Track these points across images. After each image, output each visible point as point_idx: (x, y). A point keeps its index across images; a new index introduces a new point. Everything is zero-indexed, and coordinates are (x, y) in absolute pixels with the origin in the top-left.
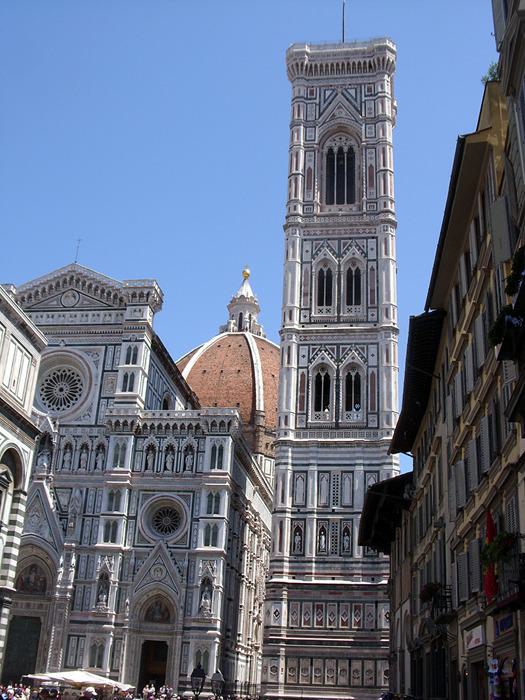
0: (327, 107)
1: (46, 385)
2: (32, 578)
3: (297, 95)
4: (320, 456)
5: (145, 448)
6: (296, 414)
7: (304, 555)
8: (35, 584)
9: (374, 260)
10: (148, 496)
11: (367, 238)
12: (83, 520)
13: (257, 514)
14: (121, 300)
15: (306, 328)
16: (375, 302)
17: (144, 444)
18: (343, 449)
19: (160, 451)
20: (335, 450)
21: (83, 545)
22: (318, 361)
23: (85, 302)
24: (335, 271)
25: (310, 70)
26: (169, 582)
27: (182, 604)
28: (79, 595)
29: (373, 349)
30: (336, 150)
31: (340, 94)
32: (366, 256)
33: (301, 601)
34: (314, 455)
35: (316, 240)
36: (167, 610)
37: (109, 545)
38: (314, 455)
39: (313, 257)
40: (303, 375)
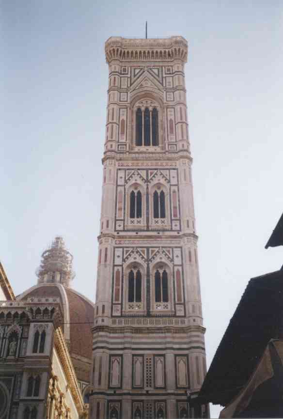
0: (137, 79)
3: (113, 70)
4: (133, 340)
6: (112, 304)
15: (121, 234)
16: (176, 216)
18: (154, 335)
20: (147, 335)
22: (131, 260)
24: (143, 191)
25: (123, 55)
29: (177, 252)
30: (143, 109)
31: (146, 71)
32: (169, 182)
35: (128, 169)
38: (129, 340)
39: (126, 182)
40: (118, 272)
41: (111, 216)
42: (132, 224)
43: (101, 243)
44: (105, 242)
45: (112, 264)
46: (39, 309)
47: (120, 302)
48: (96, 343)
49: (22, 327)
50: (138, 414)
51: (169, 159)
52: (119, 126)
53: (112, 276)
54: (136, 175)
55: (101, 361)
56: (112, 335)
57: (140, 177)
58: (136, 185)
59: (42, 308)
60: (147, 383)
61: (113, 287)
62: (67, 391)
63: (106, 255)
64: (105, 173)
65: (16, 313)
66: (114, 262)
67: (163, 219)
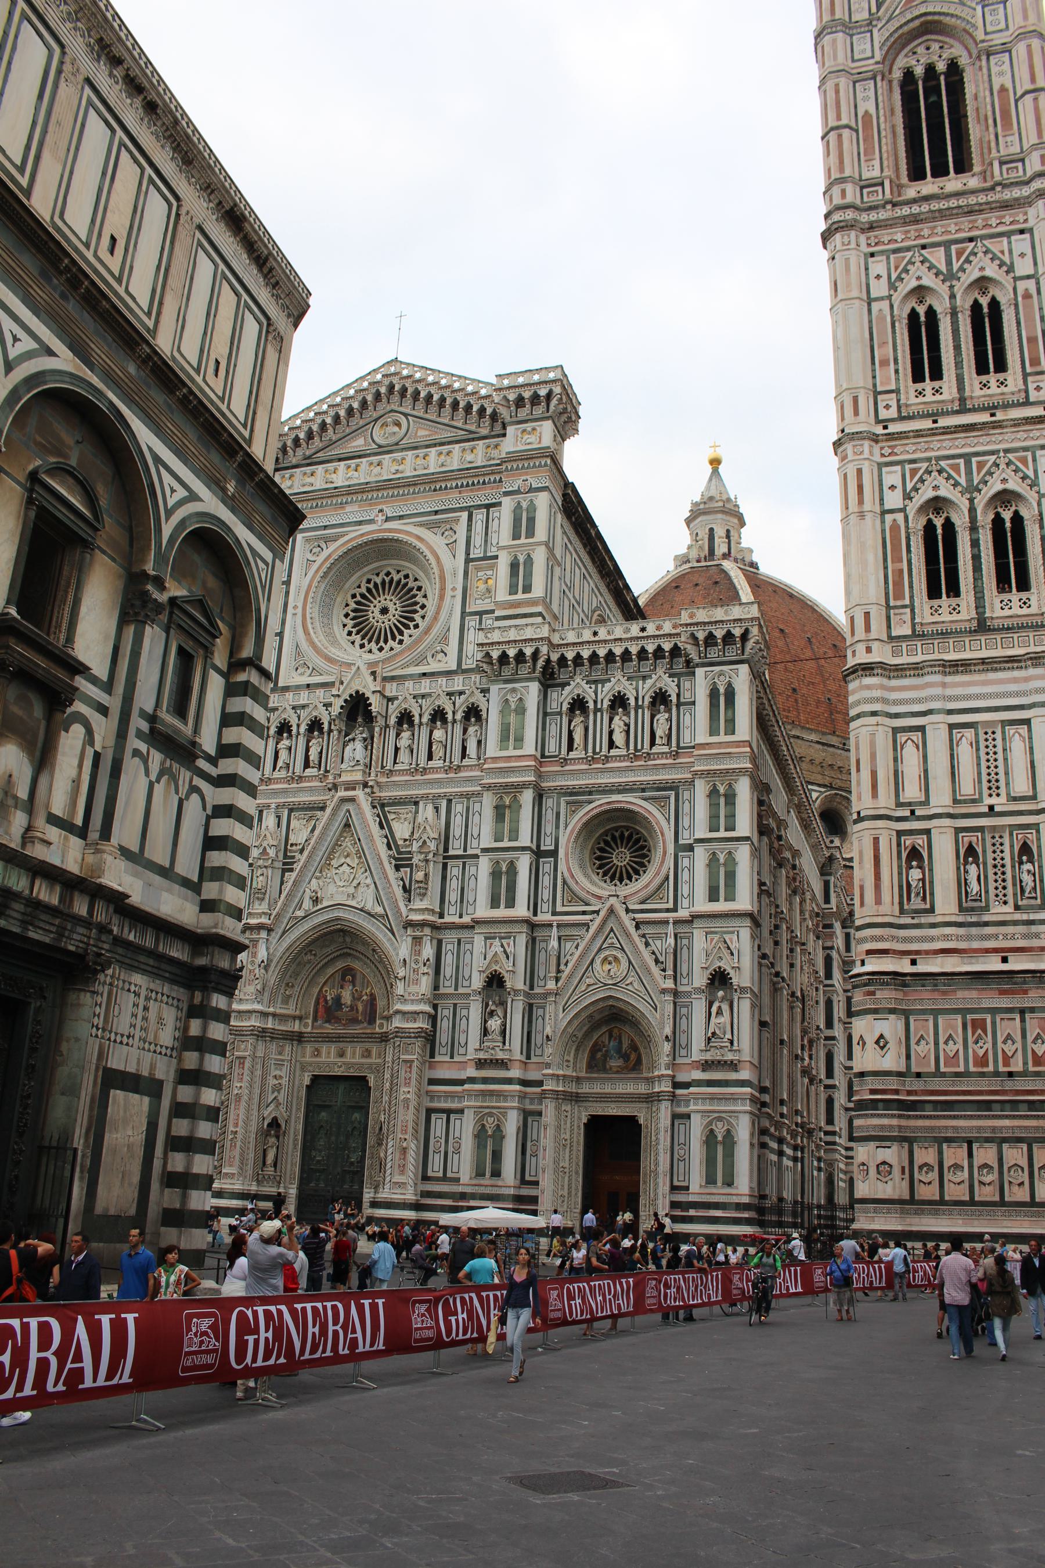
1: (353, 606)
2: (347, 997)
4: (949, 692)
5: (566, 706)
6: (888, 607)
7: (932, 910)
8: (352, 1008)
9: (1028, 277)
10: (580, 804)
11: (1008, 234)
12: (445, 866)
13: (796, 853)
14: (494, 417)
15: (893, 428)
17: (560, 699)
18: (1000, 675)
19: (596, 710)
20: (982, 677)
21: (447, 919)
22: (927, 493)
23: (421, 433)
24: (941, 307)
26: (635, 984)
27: (668, 1030)
28: (444, 1025)
32: (1010, 269)
33: (936, 1013)
34: (938, 691)
35: (895, 251)
36: (634, 1048)
37: (502, 912)
38: (938, 691)
39: (892, 286)
40: (895, 526)
41: (861, 379)
42: (921, 399)
43: (844, 458)
44: (855, 453)
45: (878, 509)
46: (710, 639)
47: (907, 602)
48: (858, 703)
49: (676, 680)
50: (970, 859)
51: (1006, 206)
52: (857, 131)
53: (880, 541)
54: (918, 264)
55: (873, 744)
56: (894, 683)
57: (929, 269)
58: (920, 292)
59: (719, 634)
60: (990, 788)
61: (886, 568)
62: (789, 812)
63: (860, 488)
64: (833, 272)
65: (659, 648)
66: (882, 503)
67: (1001, 376)
